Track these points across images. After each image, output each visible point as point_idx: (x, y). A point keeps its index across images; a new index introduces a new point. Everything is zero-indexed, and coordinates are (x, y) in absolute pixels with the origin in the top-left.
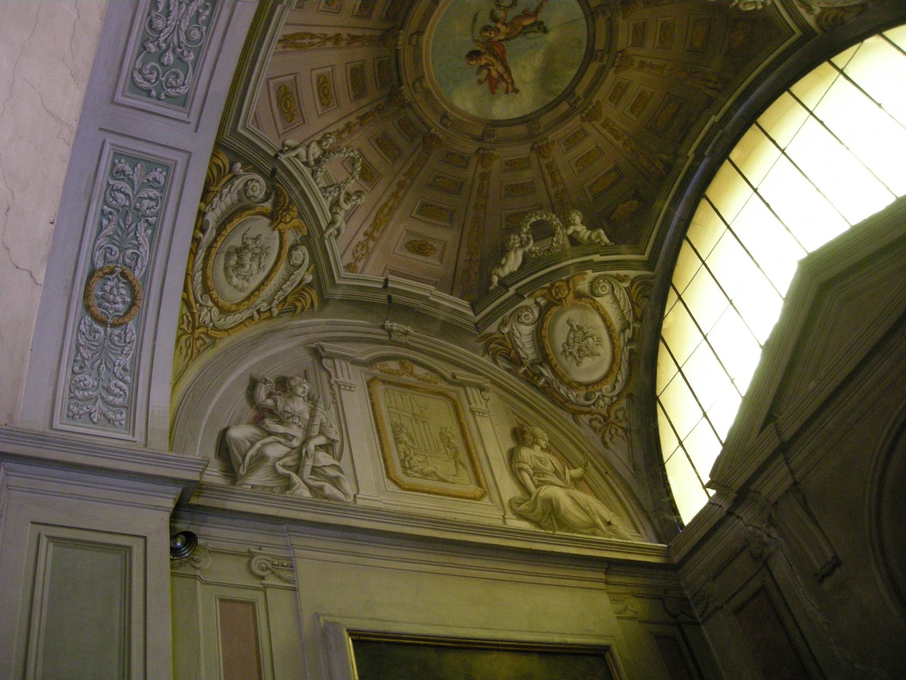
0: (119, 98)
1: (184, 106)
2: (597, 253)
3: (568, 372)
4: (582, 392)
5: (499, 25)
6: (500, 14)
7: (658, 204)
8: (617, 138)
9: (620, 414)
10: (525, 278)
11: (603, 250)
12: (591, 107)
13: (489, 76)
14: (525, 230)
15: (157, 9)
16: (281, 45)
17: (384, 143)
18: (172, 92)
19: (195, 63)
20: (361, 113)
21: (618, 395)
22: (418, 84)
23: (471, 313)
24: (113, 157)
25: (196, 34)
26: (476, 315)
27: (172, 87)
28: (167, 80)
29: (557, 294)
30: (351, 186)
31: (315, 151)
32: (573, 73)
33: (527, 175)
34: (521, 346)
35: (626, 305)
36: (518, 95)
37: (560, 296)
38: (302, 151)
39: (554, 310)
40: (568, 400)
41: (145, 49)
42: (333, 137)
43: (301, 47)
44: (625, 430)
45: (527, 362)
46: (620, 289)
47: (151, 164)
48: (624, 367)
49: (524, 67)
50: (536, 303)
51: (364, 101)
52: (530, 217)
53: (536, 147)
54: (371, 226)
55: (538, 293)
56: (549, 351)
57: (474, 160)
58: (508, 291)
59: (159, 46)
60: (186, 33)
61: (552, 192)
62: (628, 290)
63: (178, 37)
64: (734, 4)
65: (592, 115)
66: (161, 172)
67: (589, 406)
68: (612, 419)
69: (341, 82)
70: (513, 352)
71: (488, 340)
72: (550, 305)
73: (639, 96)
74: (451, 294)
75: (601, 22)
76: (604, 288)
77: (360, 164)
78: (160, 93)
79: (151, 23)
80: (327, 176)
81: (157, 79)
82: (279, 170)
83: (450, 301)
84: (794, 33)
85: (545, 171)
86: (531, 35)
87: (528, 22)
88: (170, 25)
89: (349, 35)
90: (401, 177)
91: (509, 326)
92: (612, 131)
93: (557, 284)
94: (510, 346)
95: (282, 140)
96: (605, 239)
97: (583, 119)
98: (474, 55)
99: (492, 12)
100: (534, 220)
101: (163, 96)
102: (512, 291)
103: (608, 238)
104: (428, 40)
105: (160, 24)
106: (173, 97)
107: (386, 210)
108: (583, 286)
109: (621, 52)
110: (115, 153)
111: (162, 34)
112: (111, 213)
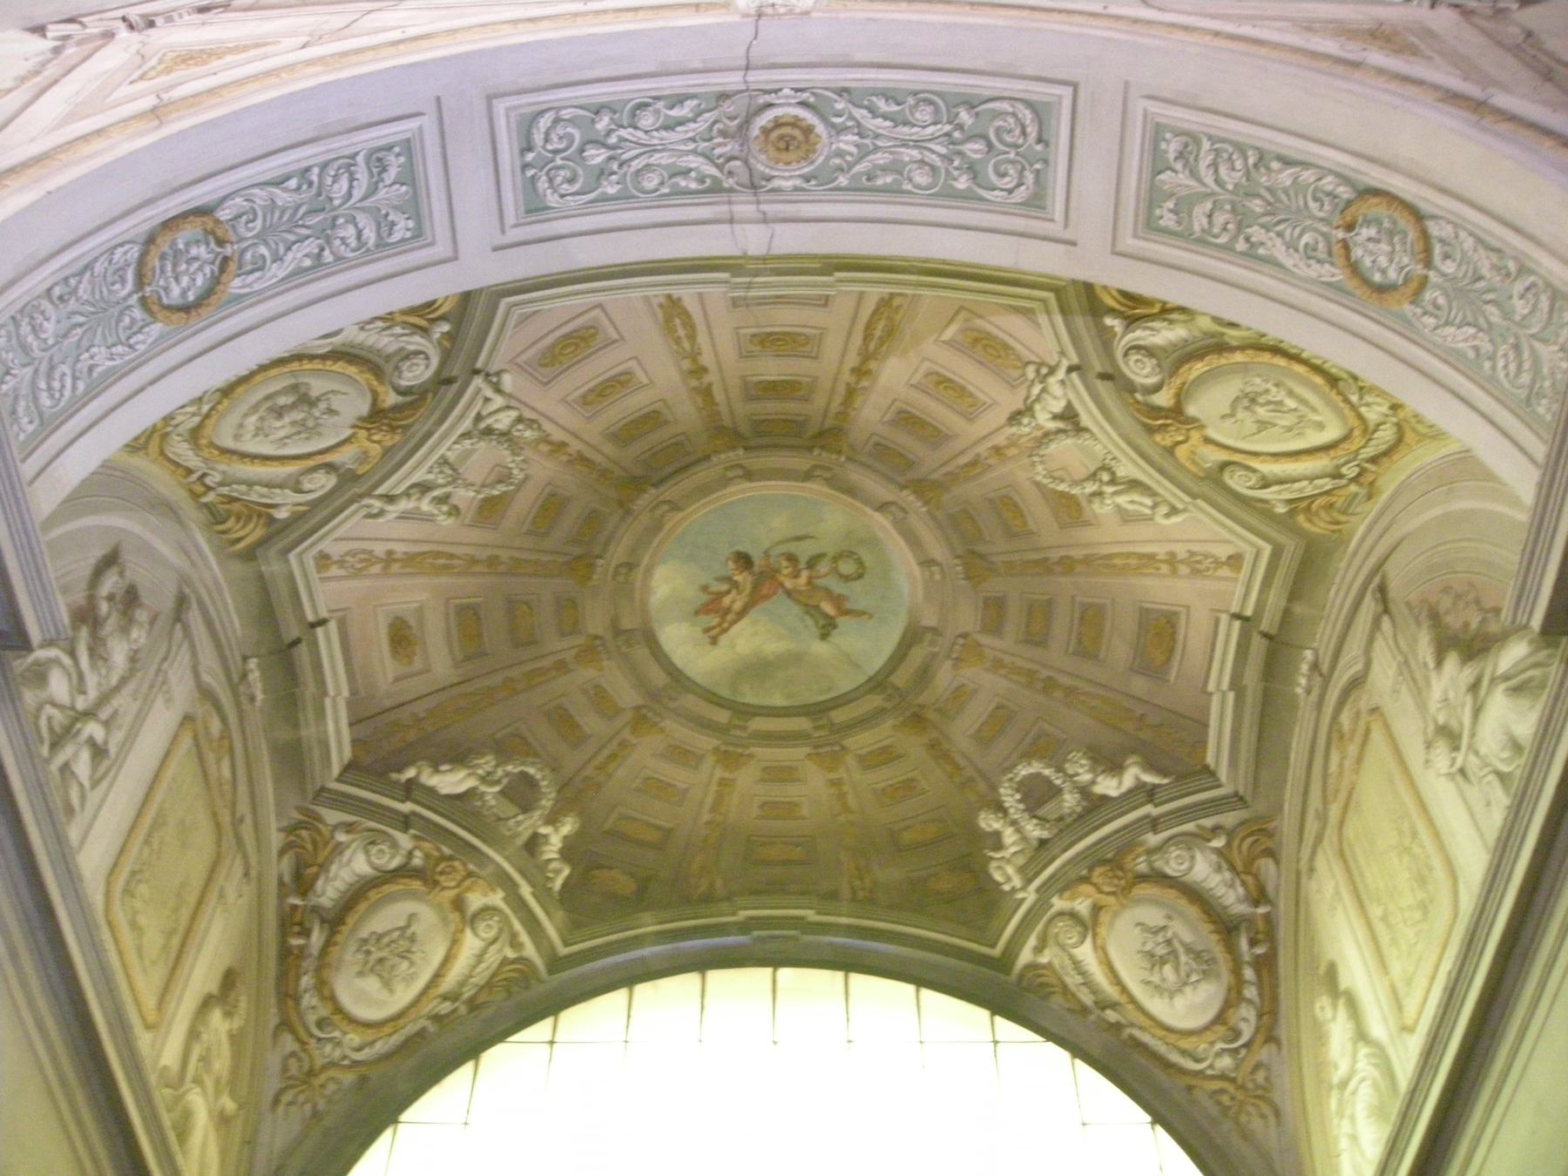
0: (500, 106)
1: (528, 211)
2: (533, 885)
3: (338, 969)
4: (324, 1011)
5: (805, 574)
6: (823, 567)
7: (647, 917)
8: (713, 809)
9: (332, 1087)
10: (442, 815)
11: (542, 892)
12: (740, 750)
13: (720, 595)
14: (510, 768)
15: (671, 108)
16: (662, 300)
17: (552, 506)
18: (542, 184)
19: (606, 198)
20: (588, 453)
21: (355, 1063)
22: (666, 507)
23: (336, 770)
24: (401, 141)
25: (651, 181)
26: (338, 780)
27: (551, 180)
28: (558, 168)
29: (441, 873)
30: (464, 496)
31: (503, 421)
32: (778, 700)
33: (592, 723)
34: (331, 875)
35: (480, 978)
36: (709, 647)
37: (442, 879)
38: (499, 401)
39: (417, 885)
40: (297, 999)
41: (597, 113)
42: (536, 434)
43: (668, 328)
44: (316, 1114)
45: (314, 900)
46: (500, 951)
47: (414, 207)
48: (396, 1039)
49: (755, 634)
50: (410, 854)
51: (609, 449)
52: (533, 764)
53: (644, 711)
54: (405, 553)
55: (427, 846)
56: (351, 920)
57: (580, 640)
58: (403, 801)
59: (609, 133)
60: (648, 165)
61: (589, 771)
62: (505, 962)
63: (637, 157)
64: (992, 854)
65: (728, 759)
66: (408, 230)
67: (312, 1035)
68: (317, 1082)
69: (634, 403)
70: (314, 869)
71: (310, 821)
72: (418, 874)
73: (789, 803)
74: (351, 725)
75: (875, 701)
76: (487, 929)
77: (504, 489)
78: (533, 167)
79: (642, 106)
80: (467, 455)
81: (556, 152)
82: (455, 387)
83: (338, 732)
84: (993, 946)
85: (615, 743)
86: (810, 622)
87: (828, 608)
88: (653, 137)
89: (710, 385)
90: (504, 555)
91: (350, 837)
92: (719, 798)
93: (457, 864)
94: (320, 859)
95: (507, 367)
96: (558, 884)
97: (716, 750)
98: (744, 561)
99: (821, 556)
100: (531, 771)
101: (530, 173)
102: (407, 807)
103: (564, 885)
104: (740, 491)
105: (647, 120)
106: (535, 189)
107: (442, 561)
108: (475, 900)
109: (843, 748)
110: (408, 141)
111: (631, 130)
112: (311, 184)
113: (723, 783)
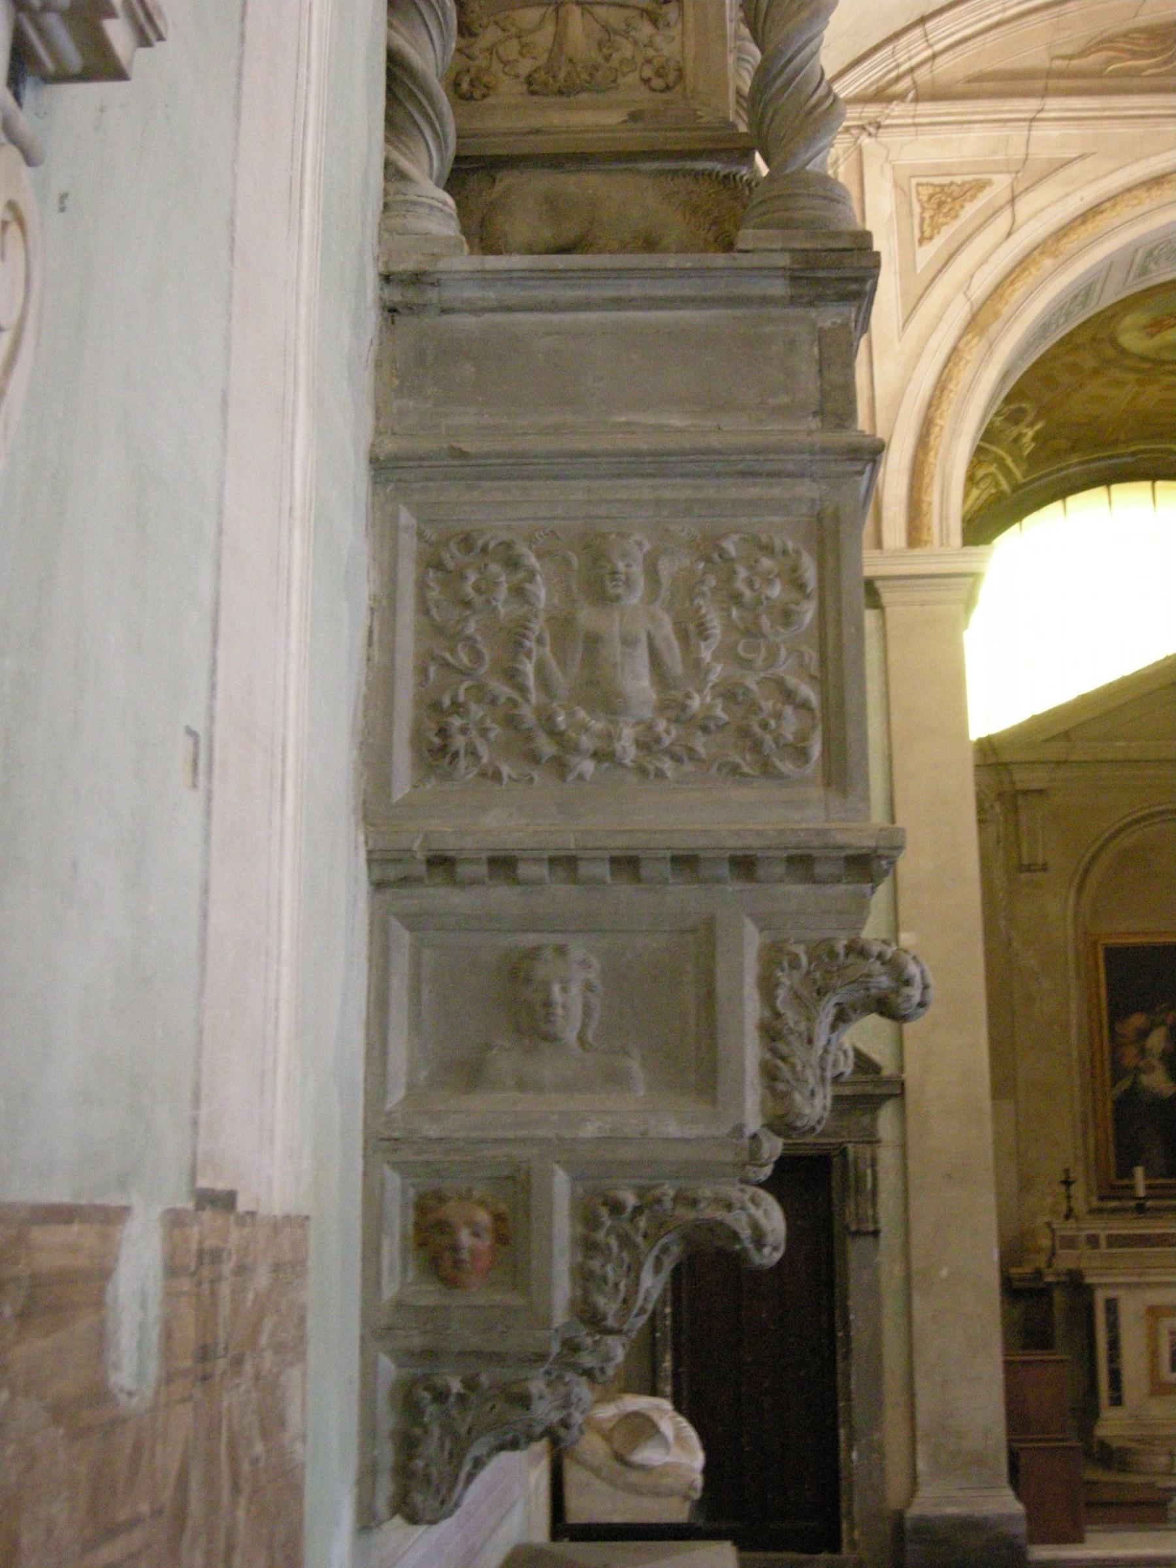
96: (1026, 452)
100: (1024, 405)
113: (1138, 393)
